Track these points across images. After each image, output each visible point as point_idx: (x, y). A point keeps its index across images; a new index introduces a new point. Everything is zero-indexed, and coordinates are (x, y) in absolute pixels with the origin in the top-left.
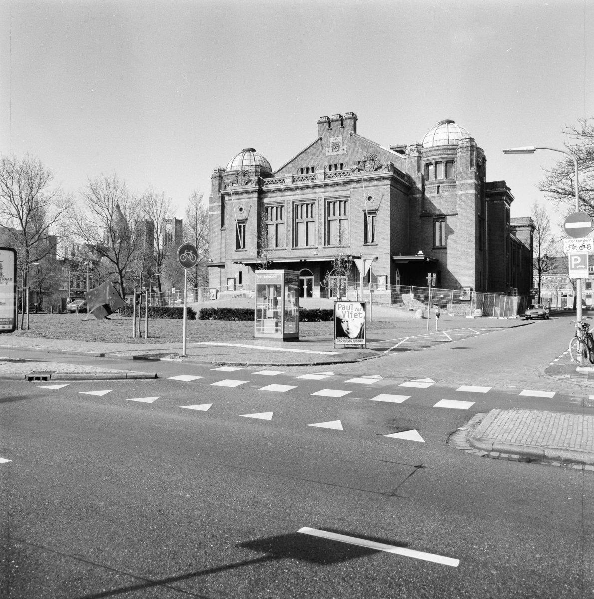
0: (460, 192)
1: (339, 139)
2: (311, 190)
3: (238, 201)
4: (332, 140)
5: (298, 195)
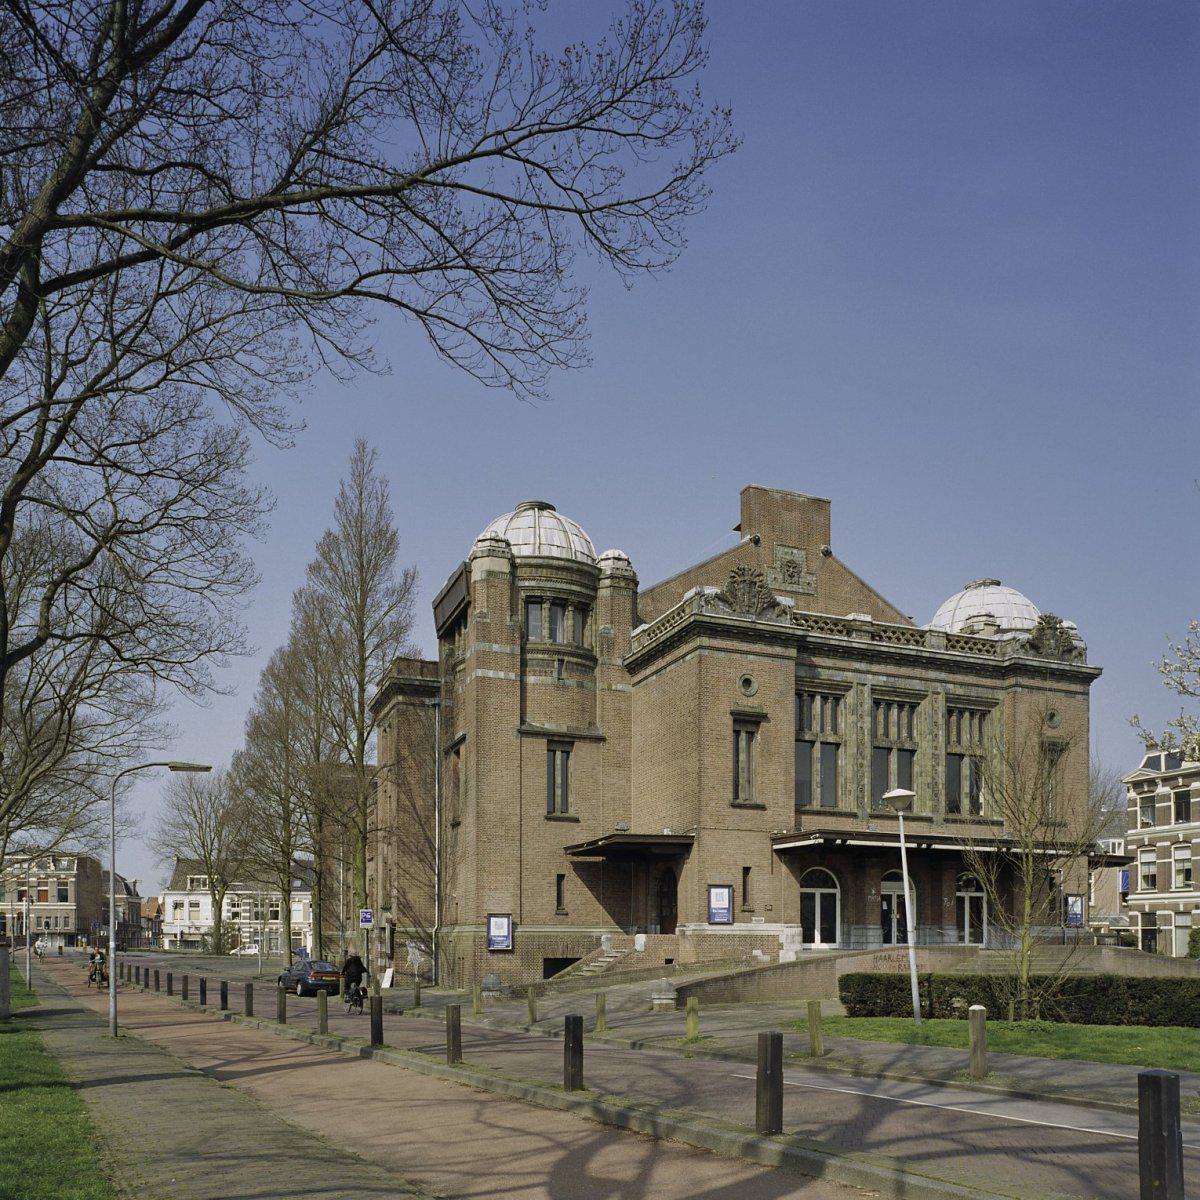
1: (799, 555)
2: (918, 672)
5: (888, 675)
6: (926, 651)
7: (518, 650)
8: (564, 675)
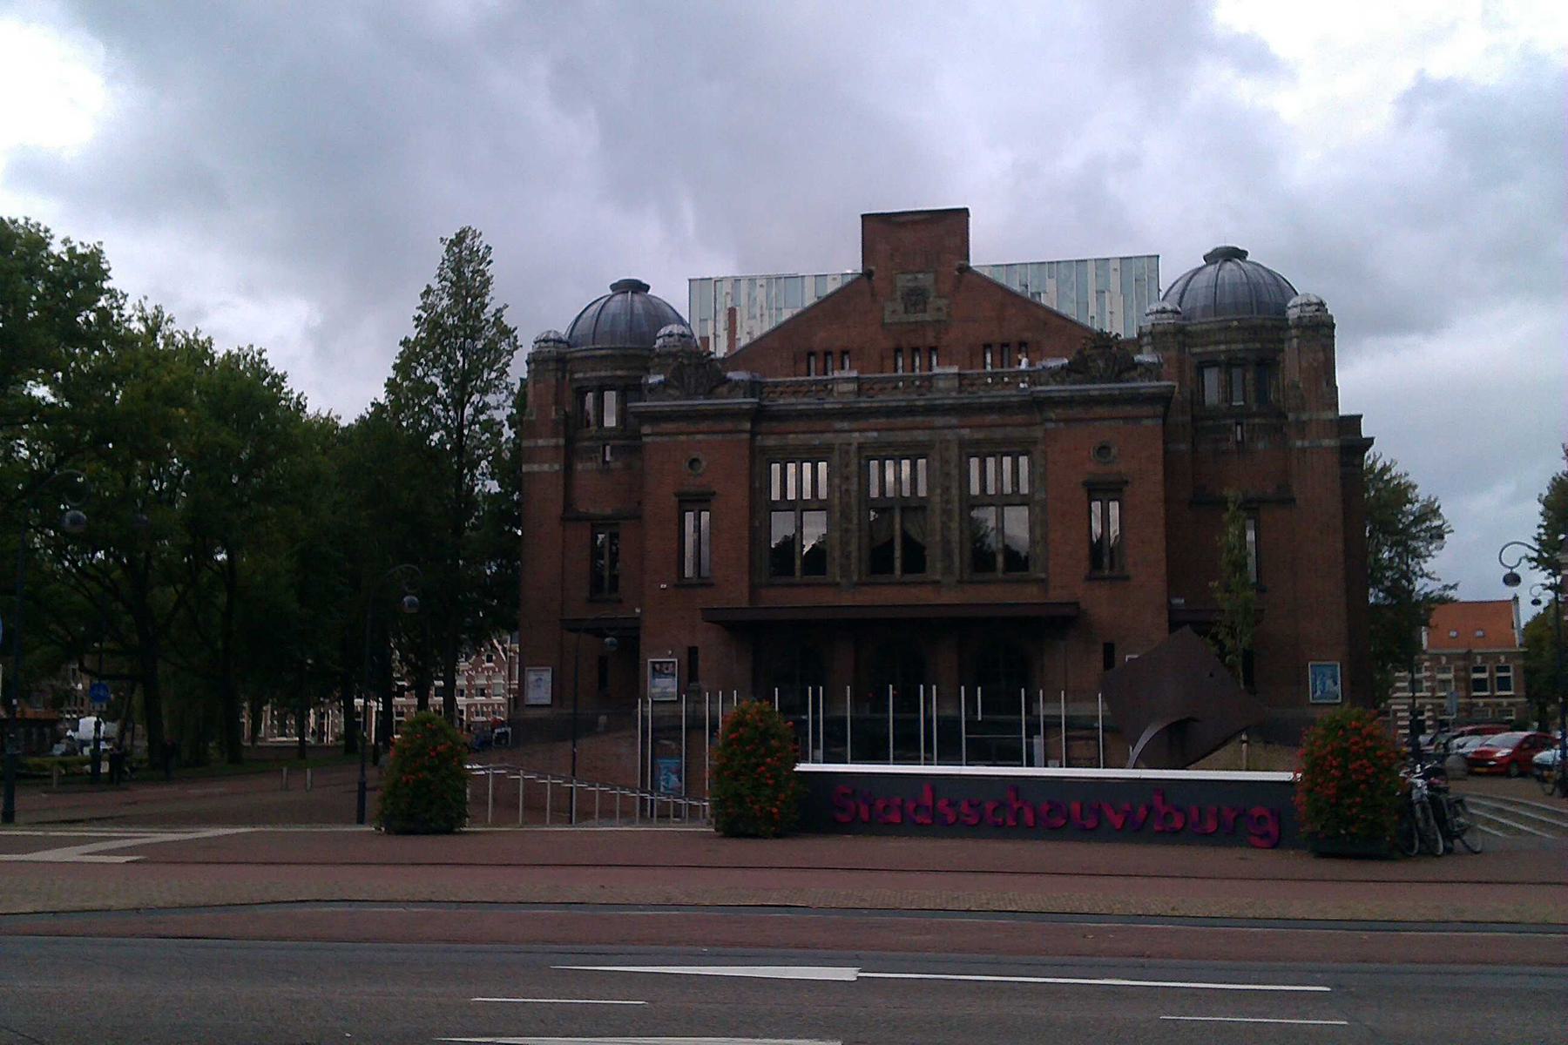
0: (1299, 443)
1: (926, 280)
4: (904, 281)
6: (936, 398)
7: (562, 441)
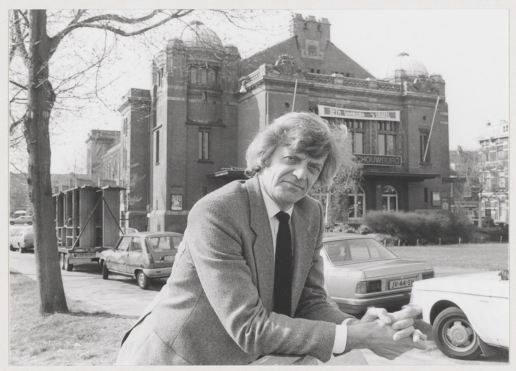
1: (316, 43)
3: (282, 93)
4: (308, 42)
7: (186, 88)
8: (208, 98)
